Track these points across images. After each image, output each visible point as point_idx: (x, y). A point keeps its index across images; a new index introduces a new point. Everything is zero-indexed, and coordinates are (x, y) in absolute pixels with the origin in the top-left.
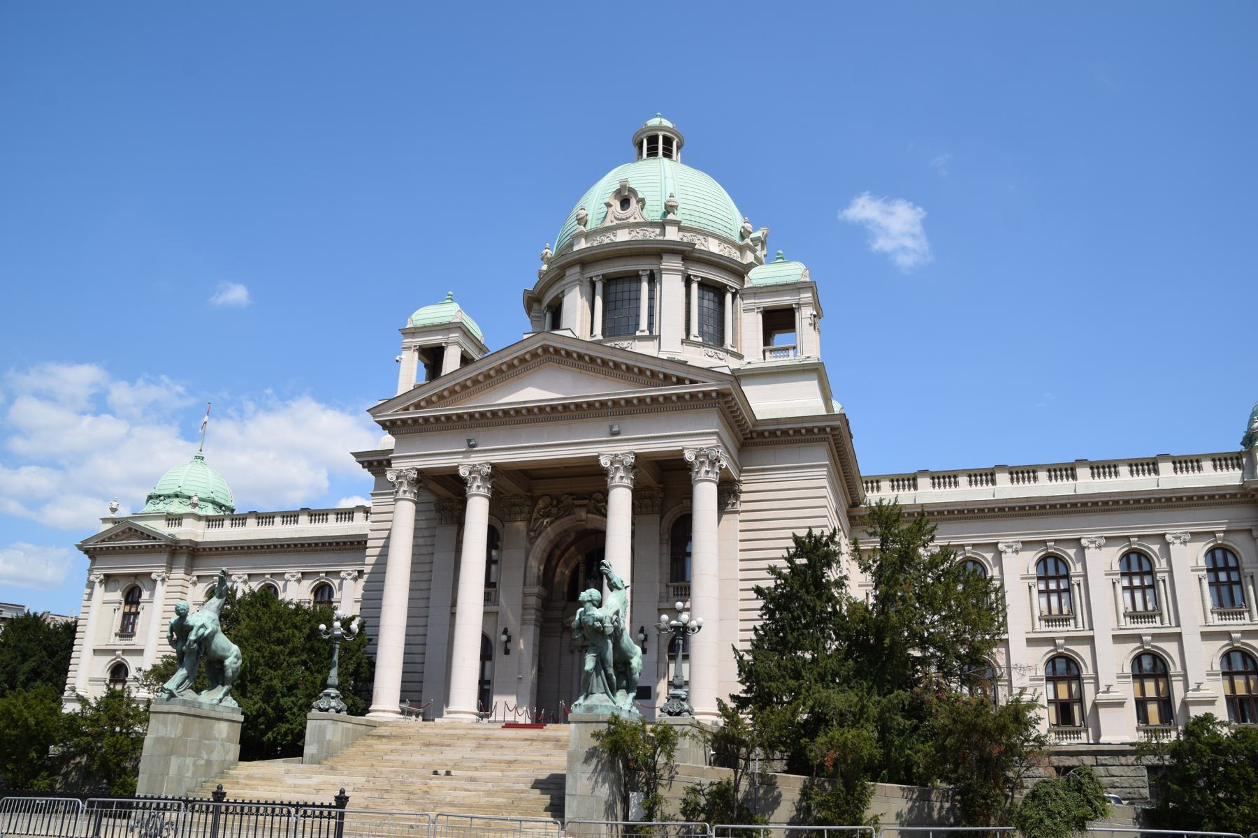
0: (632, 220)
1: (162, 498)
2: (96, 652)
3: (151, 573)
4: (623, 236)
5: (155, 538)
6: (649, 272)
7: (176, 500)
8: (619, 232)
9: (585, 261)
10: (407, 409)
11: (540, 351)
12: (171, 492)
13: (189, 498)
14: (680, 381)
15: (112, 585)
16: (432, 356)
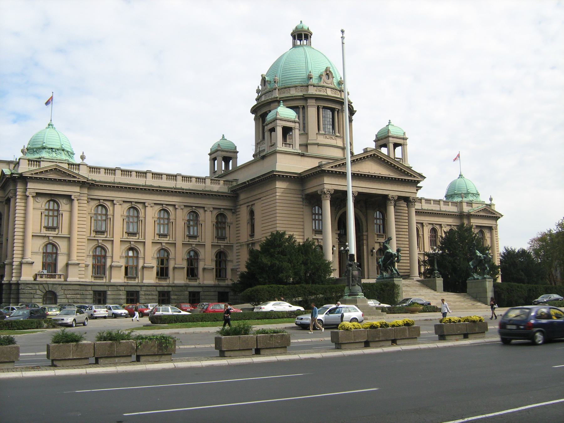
0: (330, 86)
1: (54, 150)
2: (33, 236)
3: (71, 196)
4: (329, 93)
5: (74, 177)
6: (338, 110)
7: (63, 152)
8: (327, 89)
9: (318, 98)
10: (332, 167)
11: (373, 155)
12: (58, 147)
13: (68, 152)
14: (411, 175)
15: (39, 199)
16: (287, 131)
